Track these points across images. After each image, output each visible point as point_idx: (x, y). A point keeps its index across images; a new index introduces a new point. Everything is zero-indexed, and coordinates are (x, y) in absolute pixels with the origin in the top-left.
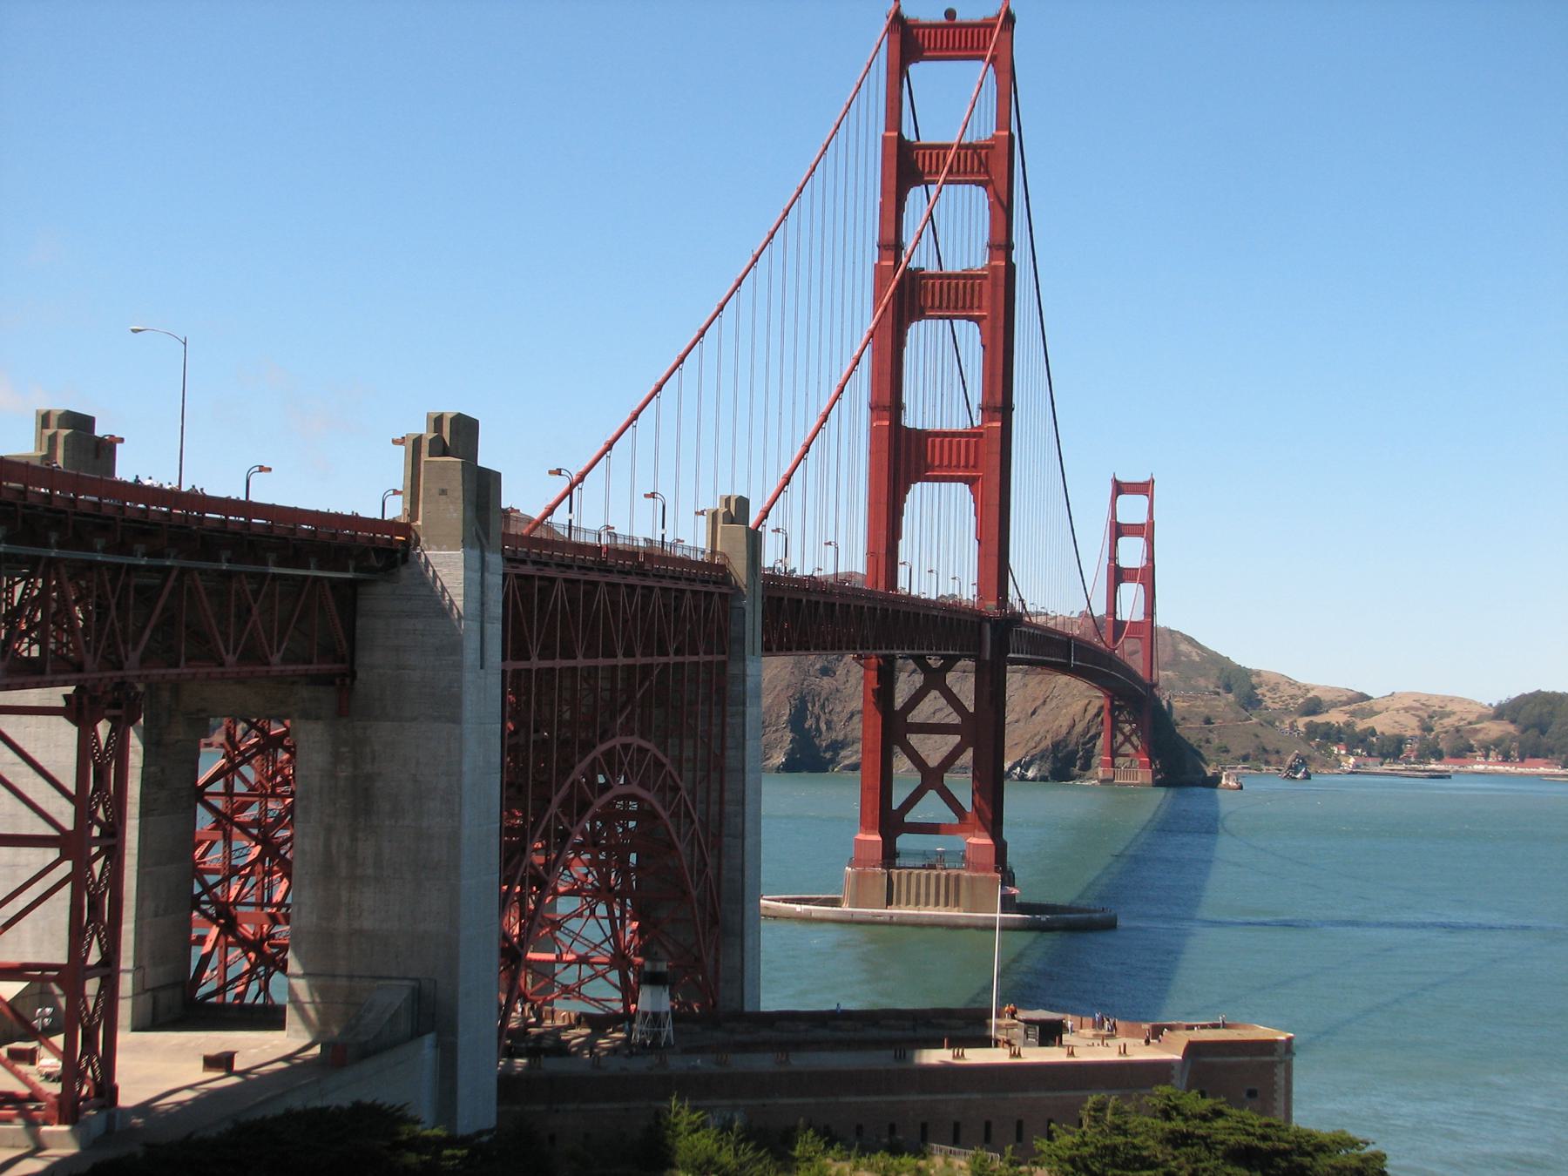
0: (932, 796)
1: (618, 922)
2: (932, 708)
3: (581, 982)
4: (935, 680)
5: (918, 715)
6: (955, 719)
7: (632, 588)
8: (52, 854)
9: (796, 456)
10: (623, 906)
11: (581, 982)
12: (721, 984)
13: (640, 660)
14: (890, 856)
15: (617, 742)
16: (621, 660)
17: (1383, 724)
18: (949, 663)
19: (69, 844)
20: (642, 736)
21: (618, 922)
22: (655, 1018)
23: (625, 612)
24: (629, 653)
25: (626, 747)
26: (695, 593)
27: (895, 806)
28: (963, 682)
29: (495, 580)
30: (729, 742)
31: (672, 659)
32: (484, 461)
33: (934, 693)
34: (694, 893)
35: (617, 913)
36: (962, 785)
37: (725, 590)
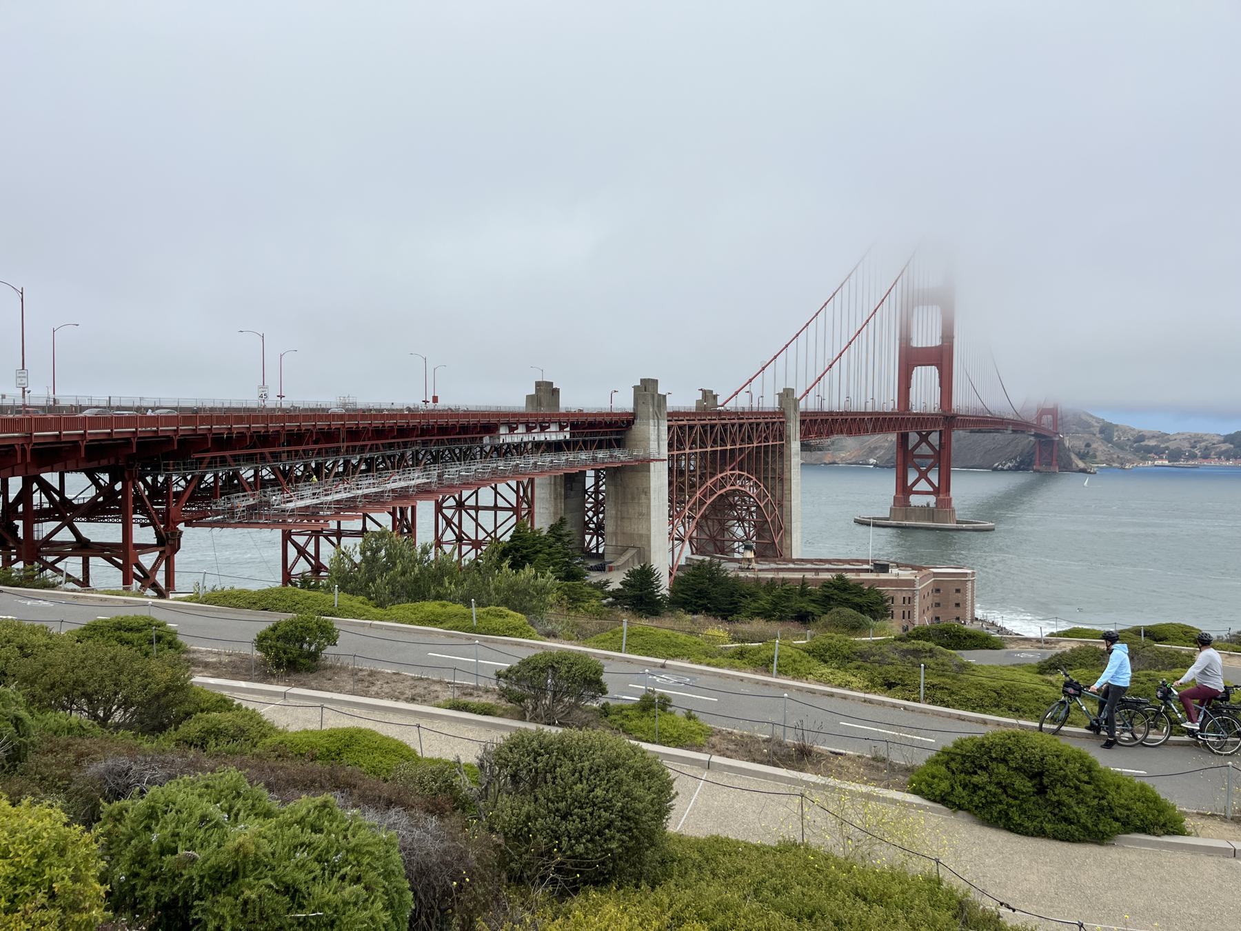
0: (923, 480)
1: (747, 529)
2: (924, 449)
3: (738, 547)
4: (924, 438)
5: (917, 452)
6: (932, 453)
7: (733, 425)
8: (512, 513)
9: (826, 368)
10: (749, 524)
11: (738, 547)
12: (784, 549)
13: (738, 446)
14: (906, 503)
15: (729, 473)
16: (729, 447)
17: (1172, 445)
18: (929, 433)
19: (516, 510)
20: (741, 470)
21: (747, 529)
22: (749, 560)
23: (731, 432)
24: (734, 443)
25: (732, 475)
26: (766, 423)
27: (909, 484)
28: (934, 438)
29: (664, 429)
30: (785, 470)
31: (755, 445)
32: (661, 391)
33: (924, 444)
34: (769, 520)
35: (746, 525)
36: (934, 477)
37: (781, 420)
